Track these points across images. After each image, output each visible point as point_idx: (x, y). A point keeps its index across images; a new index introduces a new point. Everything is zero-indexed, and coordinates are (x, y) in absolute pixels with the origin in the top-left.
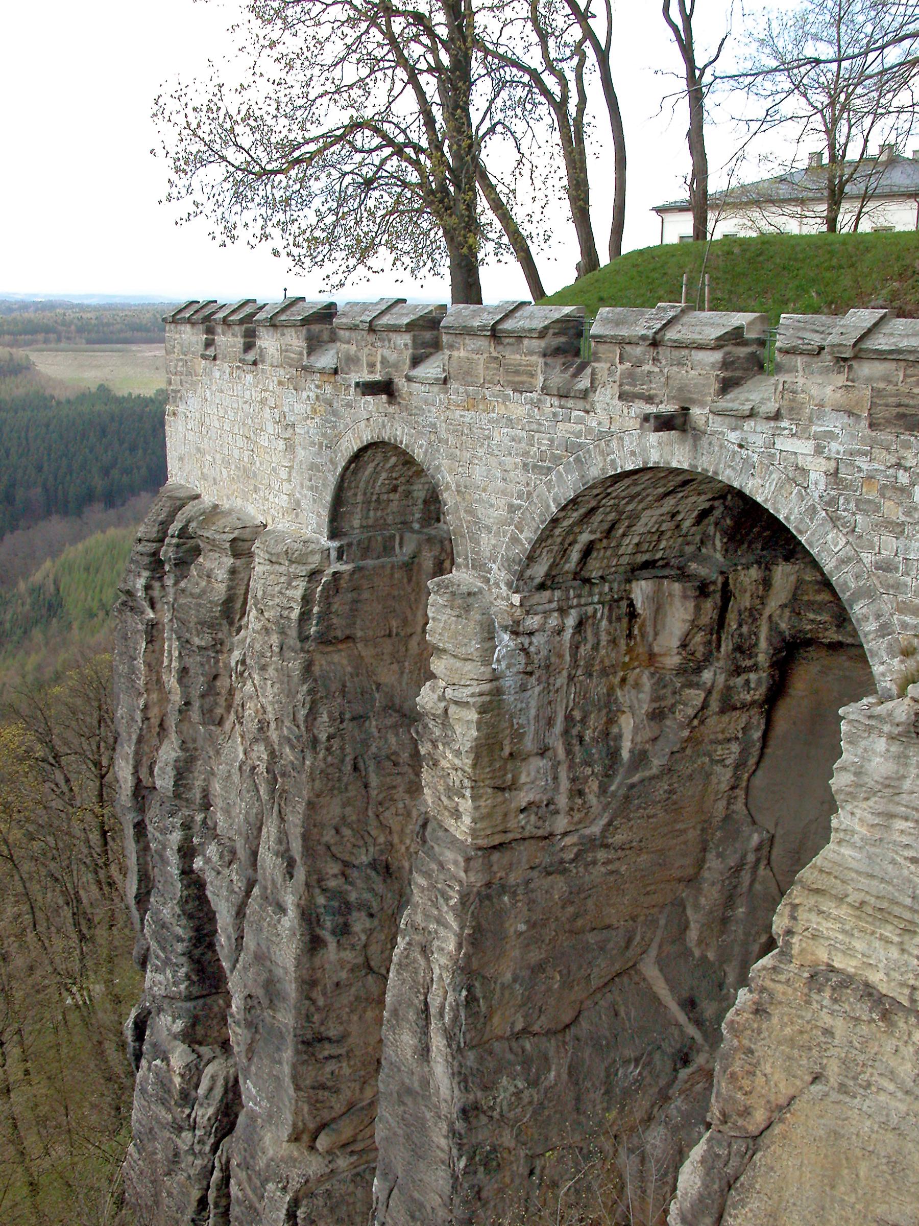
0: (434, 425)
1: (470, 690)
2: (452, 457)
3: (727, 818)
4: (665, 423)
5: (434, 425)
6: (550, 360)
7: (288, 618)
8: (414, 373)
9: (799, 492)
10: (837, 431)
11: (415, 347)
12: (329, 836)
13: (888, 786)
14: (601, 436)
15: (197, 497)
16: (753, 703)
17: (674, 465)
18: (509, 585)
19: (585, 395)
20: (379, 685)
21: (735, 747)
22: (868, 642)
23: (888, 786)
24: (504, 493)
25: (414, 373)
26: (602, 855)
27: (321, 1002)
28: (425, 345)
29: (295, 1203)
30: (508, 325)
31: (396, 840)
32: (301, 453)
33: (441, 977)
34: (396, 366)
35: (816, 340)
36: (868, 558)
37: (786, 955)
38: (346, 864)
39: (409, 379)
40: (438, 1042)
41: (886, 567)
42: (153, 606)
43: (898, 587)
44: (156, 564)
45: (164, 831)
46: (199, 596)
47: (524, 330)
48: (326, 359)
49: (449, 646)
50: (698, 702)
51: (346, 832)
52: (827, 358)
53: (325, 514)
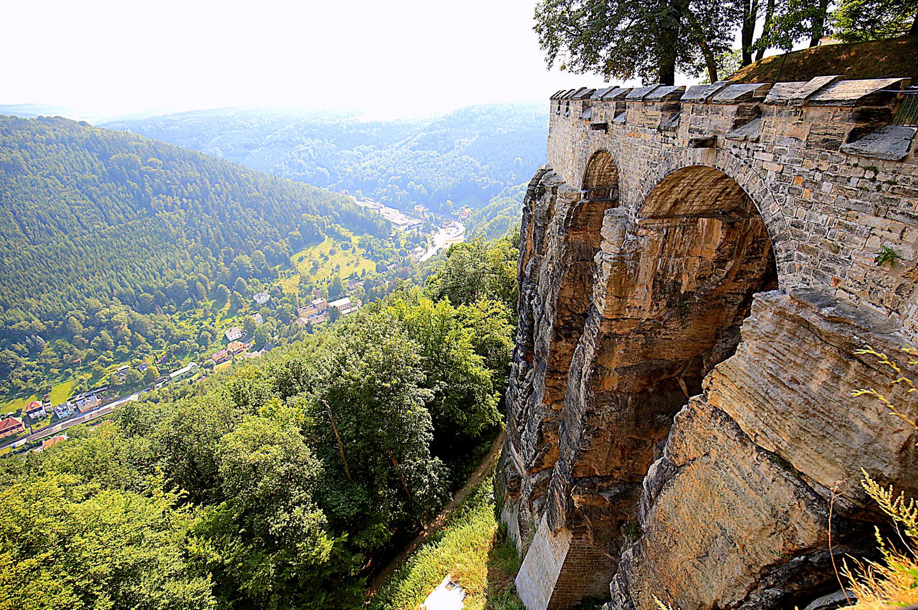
0: (619, 143)
1: (609, 257)
2: (623, 158)
4: (700, 144)
5: (619, 143)
6: (664, 113)
9: (761, 181)
10: (787, 149)
12: (568, 302)
13: (768, 337)
16: (755, 279)
20: (594, 248)
21: (741, 298)
22: (779, 263)
23: (768, 337)
26: (663, 331)
27: (558, 359)
29: (542, 423)
30: (649, 97)
37: (705, 398)
40: (583, 385)
45: (526, 289)
48: (587, 115)
49: (607, 238)
51: (574, 301)
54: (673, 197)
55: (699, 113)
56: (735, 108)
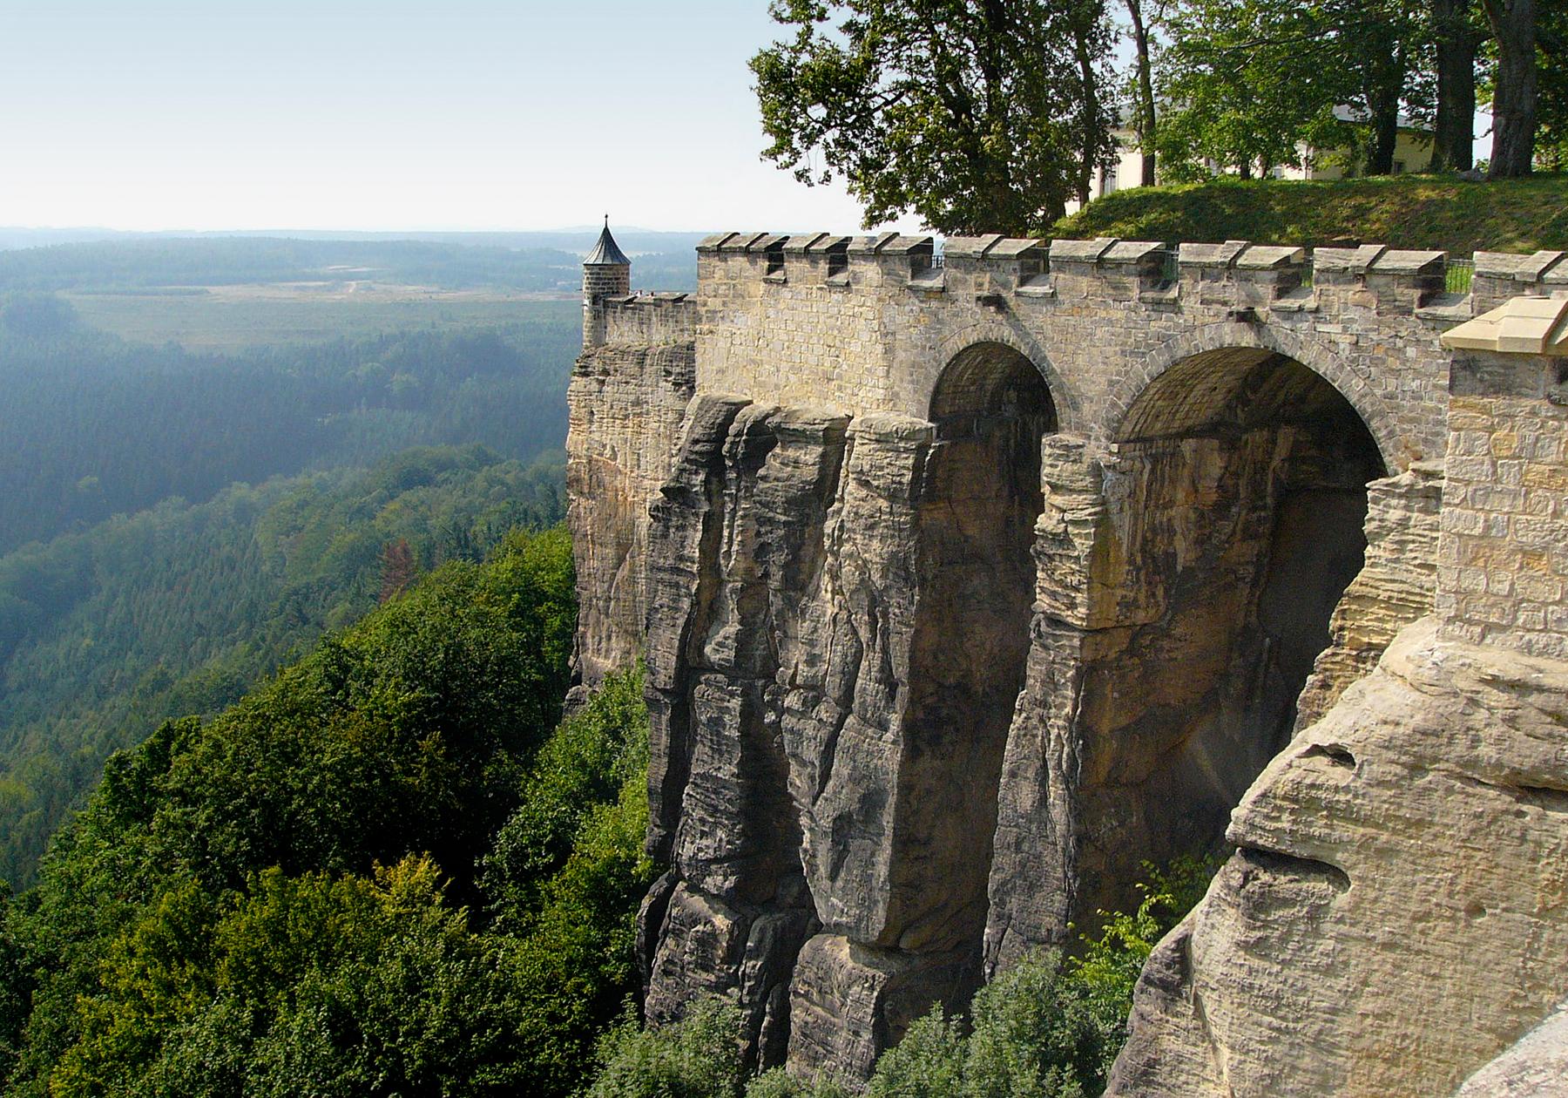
1: (1087, 512)
2: (1058, 350)
3: (1246, 627)
7: (900, 483)
8: (1020, 290)
11: (1022, 270)
12: (928, 661)
15: (750, 402)
17: (1243, 345)
18: (1108, 438)
21: (1251, 569)
24: (1104, 372)
25: (1020, 290)
28: (1029, 269)
31: (974, 667)
33: (1059, 735)
35: (1341, 264)
36: (1379, 392)
38: (940, 685)
40: (1055, 791)
41: (1391, 397)
42: (709, 499)
43: (1398, 407)
46: (788, 479)
47: (1124, 259)
50: (1228, 530)
51: (942, 658)
53: (926, 401)
55: (1217, 279)
56: (1274, 275)
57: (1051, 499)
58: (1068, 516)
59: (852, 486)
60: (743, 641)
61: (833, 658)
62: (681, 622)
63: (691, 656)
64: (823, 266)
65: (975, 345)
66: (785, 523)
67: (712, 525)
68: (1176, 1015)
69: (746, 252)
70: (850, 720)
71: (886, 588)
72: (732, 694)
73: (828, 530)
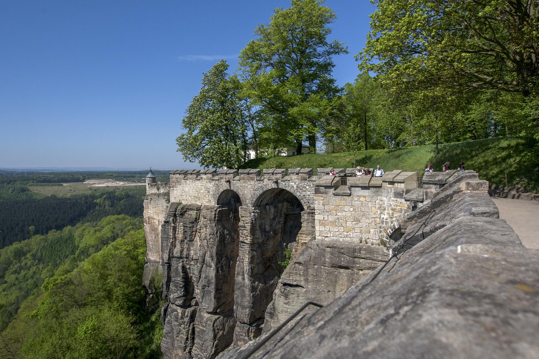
14: (265, 185)
19: (262, 180)
21: (281, 230)
29: (214, 323)
32: (211, 193)
34: (230, 178)
35: (294, 171)
36: (302, 195)
39: (233, 180)
40: (246, 276)
41: (304, 196)
43: (306, 198)
44: (175, 216)
52: (295, 173)
53: (216, 201)
54: (261, 200)
57: (241, 219)
58: (245, 222)
59: (203, 218)
60: (182, 252)
61: (200, 253)
62: (169, 248)
63: (171, 255)
64: (195, 176)
65: (225, 190)
66: (189, 227)
67: (175, 229)
68: (273, 319)
69: (180, 174)
70: (204, 266)
71: (210, 239)
72: (180, 262)
73: (198, 228)
